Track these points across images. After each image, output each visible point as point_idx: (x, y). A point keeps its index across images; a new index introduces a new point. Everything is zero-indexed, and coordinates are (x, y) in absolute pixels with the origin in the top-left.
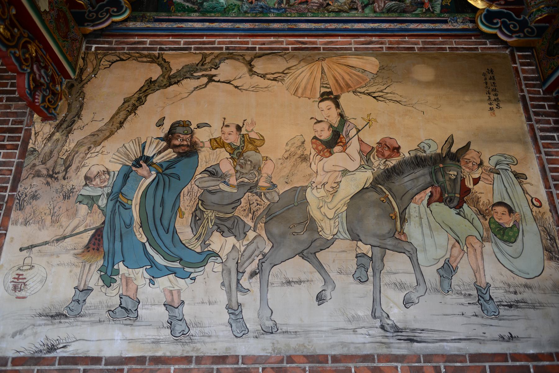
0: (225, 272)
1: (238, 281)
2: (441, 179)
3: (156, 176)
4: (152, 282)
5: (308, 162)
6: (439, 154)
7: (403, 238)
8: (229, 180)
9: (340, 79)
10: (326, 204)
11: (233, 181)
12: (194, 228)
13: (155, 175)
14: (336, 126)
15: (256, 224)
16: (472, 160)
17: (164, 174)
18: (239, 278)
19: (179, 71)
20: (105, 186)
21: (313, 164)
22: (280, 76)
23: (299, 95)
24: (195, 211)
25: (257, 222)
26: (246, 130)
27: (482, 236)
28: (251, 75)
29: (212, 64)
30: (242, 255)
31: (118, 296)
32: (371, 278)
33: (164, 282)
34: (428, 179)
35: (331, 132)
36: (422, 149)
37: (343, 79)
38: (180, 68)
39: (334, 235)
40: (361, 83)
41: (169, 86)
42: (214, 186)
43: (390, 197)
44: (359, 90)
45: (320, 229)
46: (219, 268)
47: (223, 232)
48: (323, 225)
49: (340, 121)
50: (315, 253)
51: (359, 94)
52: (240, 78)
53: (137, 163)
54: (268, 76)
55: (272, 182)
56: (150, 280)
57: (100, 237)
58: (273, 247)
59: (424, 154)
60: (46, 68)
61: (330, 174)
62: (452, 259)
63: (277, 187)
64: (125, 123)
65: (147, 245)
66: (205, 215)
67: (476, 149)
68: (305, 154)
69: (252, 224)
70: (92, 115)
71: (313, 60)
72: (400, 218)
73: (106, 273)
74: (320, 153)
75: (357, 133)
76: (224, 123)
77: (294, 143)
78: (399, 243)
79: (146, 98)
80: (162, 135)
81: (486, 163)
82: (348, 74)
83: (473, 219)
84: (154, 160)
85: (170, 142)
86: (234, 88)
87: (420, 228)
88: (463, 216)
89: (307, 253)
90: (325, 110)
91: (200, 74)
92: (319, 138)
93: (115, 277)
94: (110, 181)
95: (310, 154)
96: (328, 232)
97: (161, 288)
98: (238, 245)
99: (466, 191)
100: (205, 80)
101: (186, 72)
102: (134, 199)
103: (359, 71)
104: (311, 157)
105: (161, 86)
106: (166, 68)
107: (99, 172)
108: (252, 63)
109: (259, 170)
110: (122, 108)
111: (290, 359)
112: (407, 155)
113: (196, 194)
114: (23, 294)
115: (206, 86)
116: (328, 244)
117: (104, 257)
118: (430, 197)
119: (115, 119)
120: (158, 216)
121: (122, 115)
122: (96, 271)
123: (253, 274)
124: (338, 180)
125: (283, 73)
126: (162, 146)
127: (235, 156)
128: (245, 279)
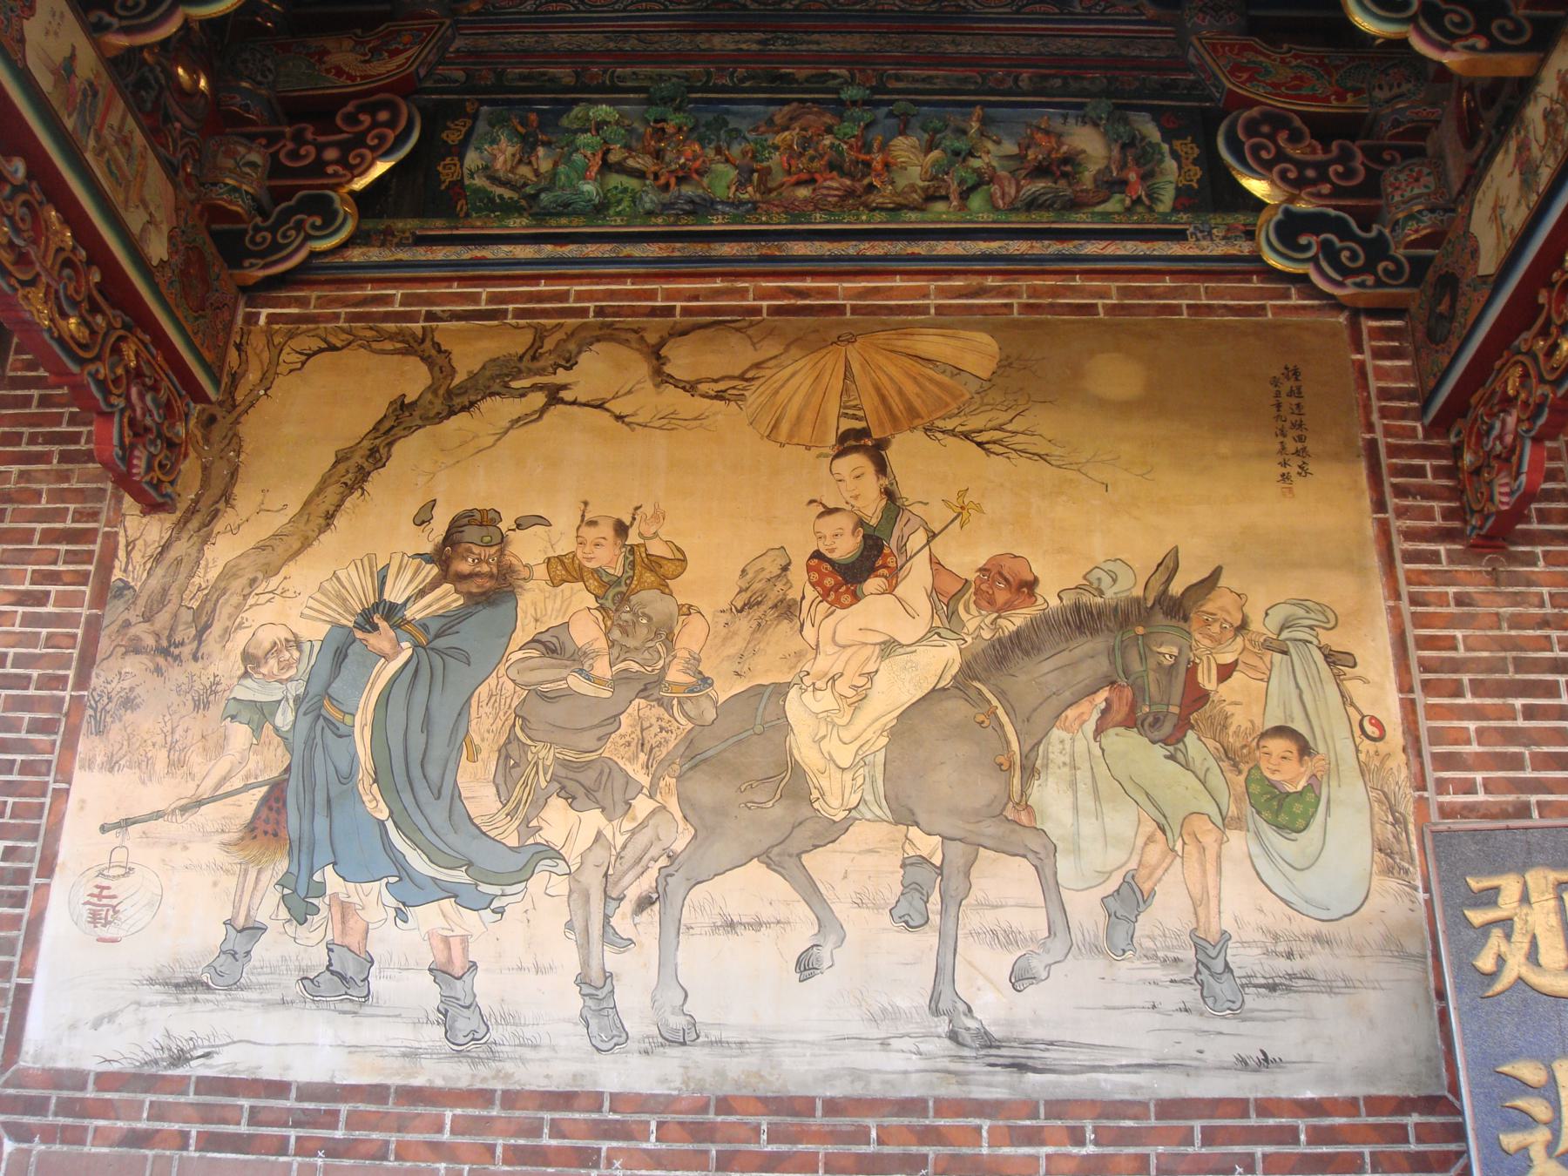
0: (575, 896)
1: (607, 918)
2: (1136, 666)
3: (412, 656)
4: (401, 915)
5: (796, 620)
6: (1137, 601)
7: (1024, 818)
8: (592, 665)
9: (894, 393)
10: (835, 732)
11: (602, 668)
12: (502, 789)
13: (410, 652)
14: (873, 522)
15: (656, 780)
16: (1220, 615)
17: (432, 649)
18: (609, 912)
19: (473, 377)
20: (290, 679)
21: (808, 625)
22: (734, 388)
23: (782, 439)
24: (505, 744)
25: (658, 775)
26: (640, 535)
27: (1224, 813)
28: (657, 386)
29: (559, 356)
30: (619, 856)
31: (323, 944)
32: (935, 919)
33: (430, 916)
34: (1103, 665)
35: (860, 538)
36: (1095, 585)
37: (901, 392)
38: (476, 368)
39: (850, 810)
40: (947, 405)
41: (448, 417)
42: (553, 681)
43: (1000, 712)
44: (940, 424)
45: (815, 794)
46: (560, 886)
47: (574, 798)
48: (825, 783)
49: (886, 509)
50: (799, 856)
51: (940, 435)
52: (630, 392)
53: (366, 622)
54: (703, 387)
55: (700, 673)
56: (397, 910)
57: (280, 805)
58: (695, 837)
59: (1099, 600)
60: (155, 388)
61: (849, 651)
62: (1143, 872)
63: (711, 685)
64: (338, 515)
65: (390, 825)
66: (530, 756)
67: (1235, 586)
68: (789, 597)
69: (645, 780)
70: (259, 498)
71: (825, 340)
72: (1023, 767)
73: (295, 891)
74: (828, 595)
75: (928, 542)
76: (583, 516)
77: (763, 569)
78: (1013, 831)
79: (389, 450)
80: (428, 548)
81: (1256, 625)
82: (915, 379)
83: (1208, 769)
84: (409, 614)
85: (448, 567)
86: (612, 421)
87: (1070, 793)
88: (1184, 763)
89: (779, 855)
90: (847, 478)
91: (526, 383)
92: (829, 556)
93: (315, 901)
94: (303, 666)
95: (803, 598)
96: (835, 803)
97: (424, 930)
98: (608, 833)
99: (1197, 698)
100: (539, 399)
101: (493, 378)
102: (360, 711)
103: (944, 372)
104: (806, 604)
105: (427, 419)
106: (441, 368)
107: (275, 643)
108: (663, 352)
109: (670, 640)
110: (330, 477)
111: (725, 1105)
112: (1054, 602)
113: (508, 700)
114: (109, 932)
115: (540, 417)
116: (831, 832)
117: (290, 853)
118: (1104, 712)
119: (313, 506)
120: (416, 756)
121: (332, 495)
122: (271, 886)
123: (644, 903)
124: (871, 667)
125: (742, 377)
126: (427, 576)
127: (609, 604)
128: (624, 915)
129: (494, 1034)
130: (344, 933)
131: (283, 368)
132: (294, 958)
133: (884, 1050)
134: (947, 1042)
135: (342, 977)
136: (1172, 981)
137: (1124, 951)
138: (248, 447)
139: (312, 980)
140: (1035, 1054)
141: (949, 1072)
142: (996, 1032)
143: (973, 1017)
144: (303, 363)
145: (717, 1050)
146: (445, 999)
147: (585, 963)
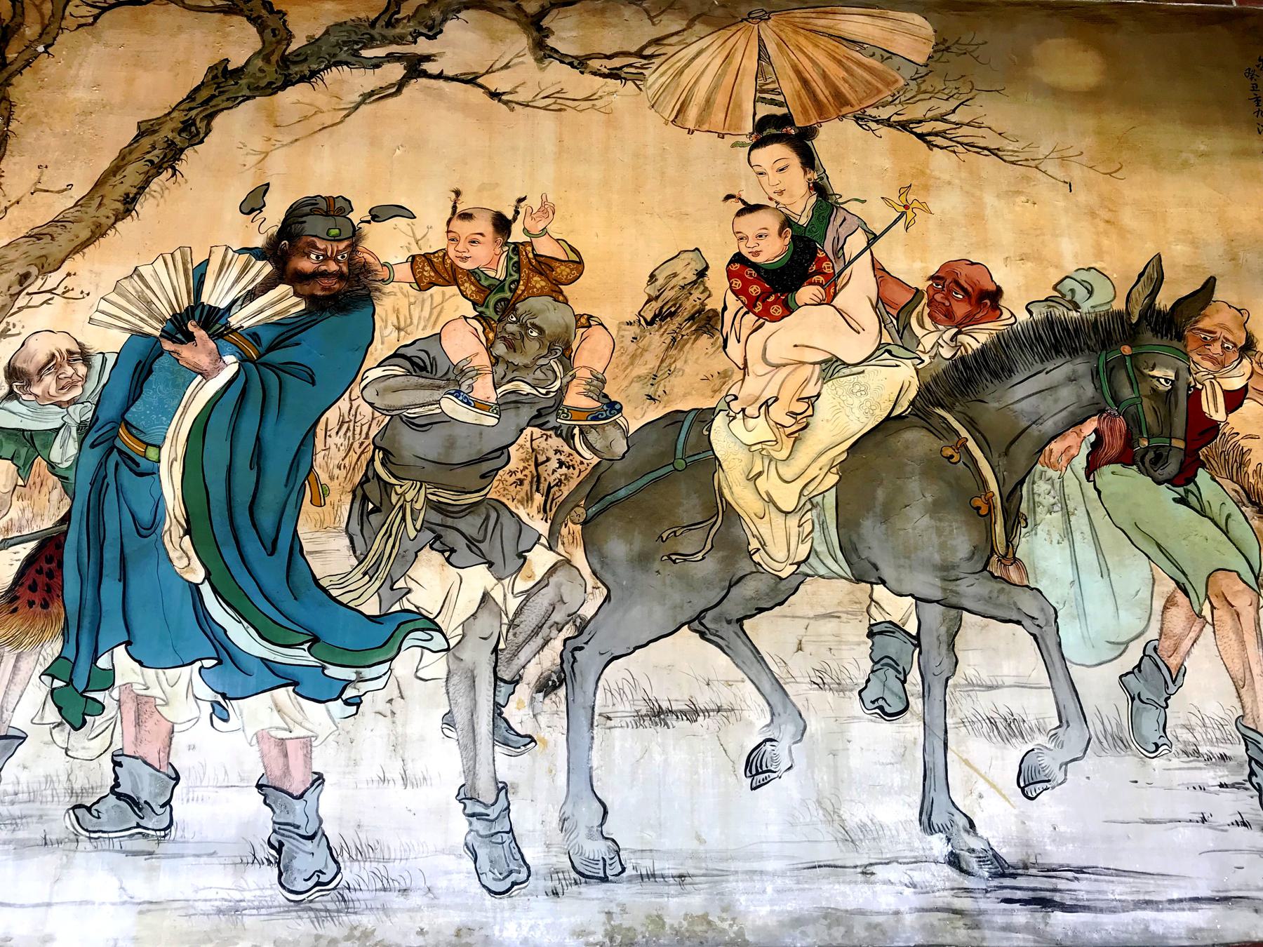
0: (455, 680)
1: (498, 709)
2: (1126, 392)
3: (238, 372)
4: (220, 712)
5: (718, 335)
6: (1119, 314)
7: (1014, 575)
8: (471, 387)
9: (816, 77)
10: (773, 464)
11: (484, 389)
12: (359, 541)
13: (235, 367)
14: (803, 221)
15: (556, 527)
16: (1220, 333)
17: (264, 364)
18: (502, 701)
19: (313, 42)
20: (73, 402)
21: (732, 341)
22: (630, 65)
23: (691, 125)
24: (361, 484)
25: (559, 520)
26: (526, 231)
27: (1257, 572)
28: (539, 60)
29: (420, 23)
30: (512, 625)
31: (108, 756)
32: (916, 704)
34: (1089, 390)
35: (788, 240)
36: (1069, 298)
37: (825, 76)
38: (318, 33)
39: (799, 564)
40: (879, 91)
41: (283, 87)
42: (423, 405)
43: (971, 444)
44: (870, 111)
45: (754, 544)
47: (452, 551)
48: (764, 528)
49: (816, 208)
50: (740, 621)
51: (873, 125)
52: (506, 67)
53: (178, 328)
54: (595, 64)
55: (606, 396)
56: (214, 704)
57: (54, 565)
58: (608, 598)
59: (1075, 314)
61: (784, 372)
62: (1166, 644)
63: (620, 411)
64: (142, 199)
65: (206, 590)
66: (394, 499)
67: (1234, 300)
68: (707, 308)
69: (543, 527)
70: (34, 174)
71: (734, 17)
72: (1005, 511)
73: (70, 683)
74: (755, 306)
75: (869, 245)
76: (454, 208)
77: (675, 275)
78: (1002, 591)
79: (209, 124)
80: (259, 242)
82: (839, 62)
83: (1229, 516)
84: (234, 321)
85: (285, 263)
86: (487, 98)
87: (1066, 543)
88: (1199, 509)
89: (716, 620)
90: (769, 172)
91: (380, 52)
92: (753, 259)
93: (98, 696)
94: (91, 385)
95: (725, 308)
96: (781, 554)
97: (250, 732)
98: (497, 595)
100: (396, 71)
101: (338, 45)
102: (168, 442)
103: (873, 55)
104: (728, 316)
105: (257, 88)
106: (273, 31)
107: (53, 356)
108: (545, 23)
109: (567, 357)
110: (130, 153)
112: (1023, 316)
113: (365, 428)
115: (399, 91)
117: (65, 632)
118: (1096, 446)
119: (107, 189)
120: (242, 498)
121: (132, 174)
122: (35, 677)
123: (546, 687)
124: (811, 391)
125: (639, 54)
126: (257, 275)
127: (490, 312)
128: (520, 702)
129: (347, 876)
130: (138, 741)
131: (69, 22)
132: (64, 778)
133: (867, 882)
134: (948, 871)
135: (133, 802)
136: (1221, 786)
137: (1157, 747)
138: (20, 114)
139: (89, 809)
140: (1062, 885)
141: (955, 912)
142: (1009, 854)
143: (976, 834)
144: (96, 18)
145: (649, 886)
146: (279, 827)
147: (471, 771)
